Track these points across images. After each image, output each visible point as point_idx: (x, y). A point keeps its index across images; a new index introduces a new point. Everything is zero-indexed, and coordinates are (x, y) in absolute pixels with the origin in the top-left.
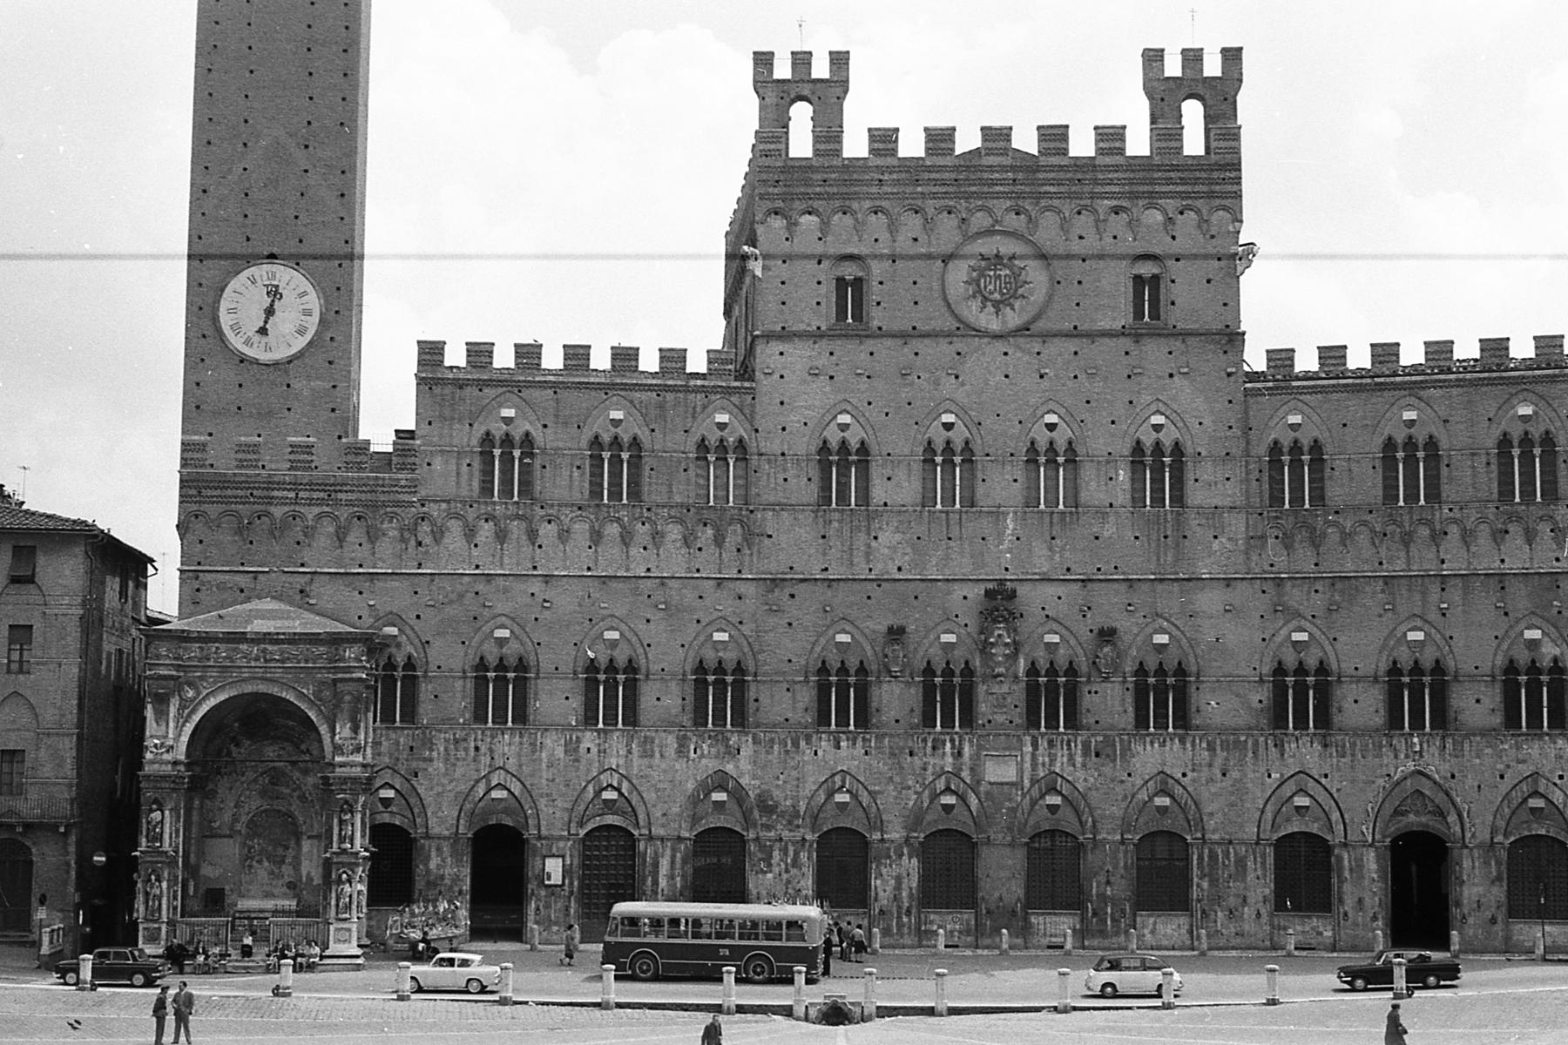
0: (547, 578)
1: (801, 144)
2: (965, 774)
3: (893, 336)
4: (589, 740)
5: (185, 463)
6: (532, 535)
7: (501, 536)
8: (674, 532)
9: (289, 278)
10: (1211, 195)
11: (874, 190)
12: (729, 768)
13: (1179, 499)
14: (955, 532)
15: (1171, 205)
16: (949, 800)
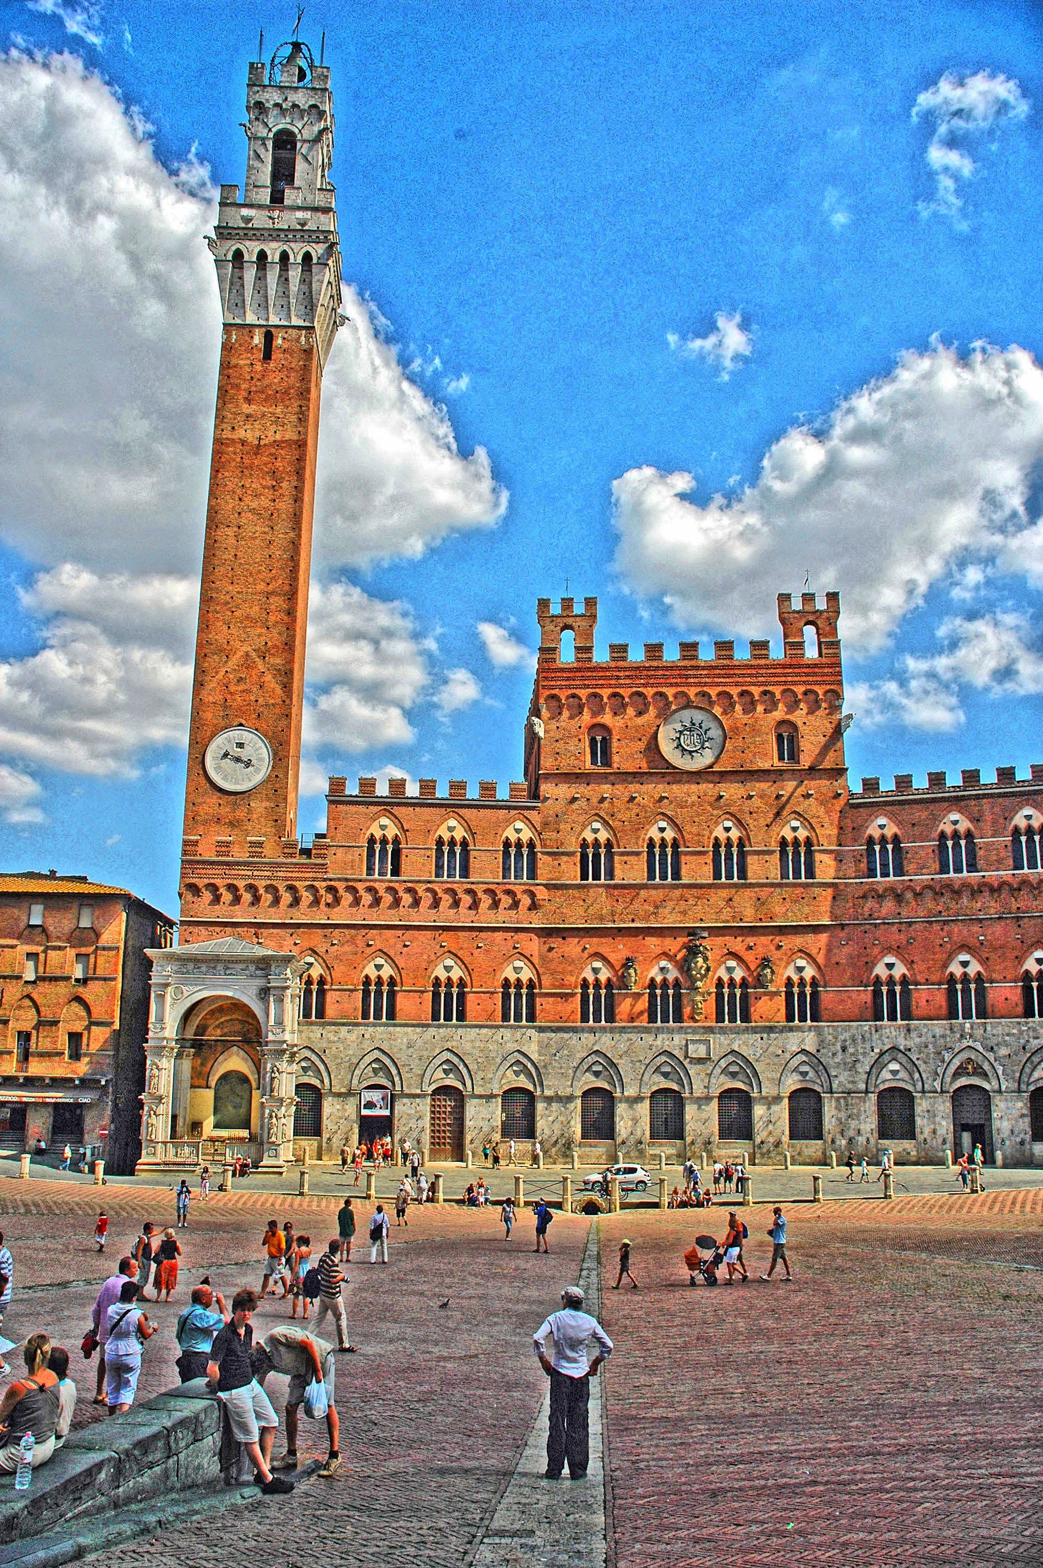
1: (567, 655)
5: (185, 853)
11: (613, 682)
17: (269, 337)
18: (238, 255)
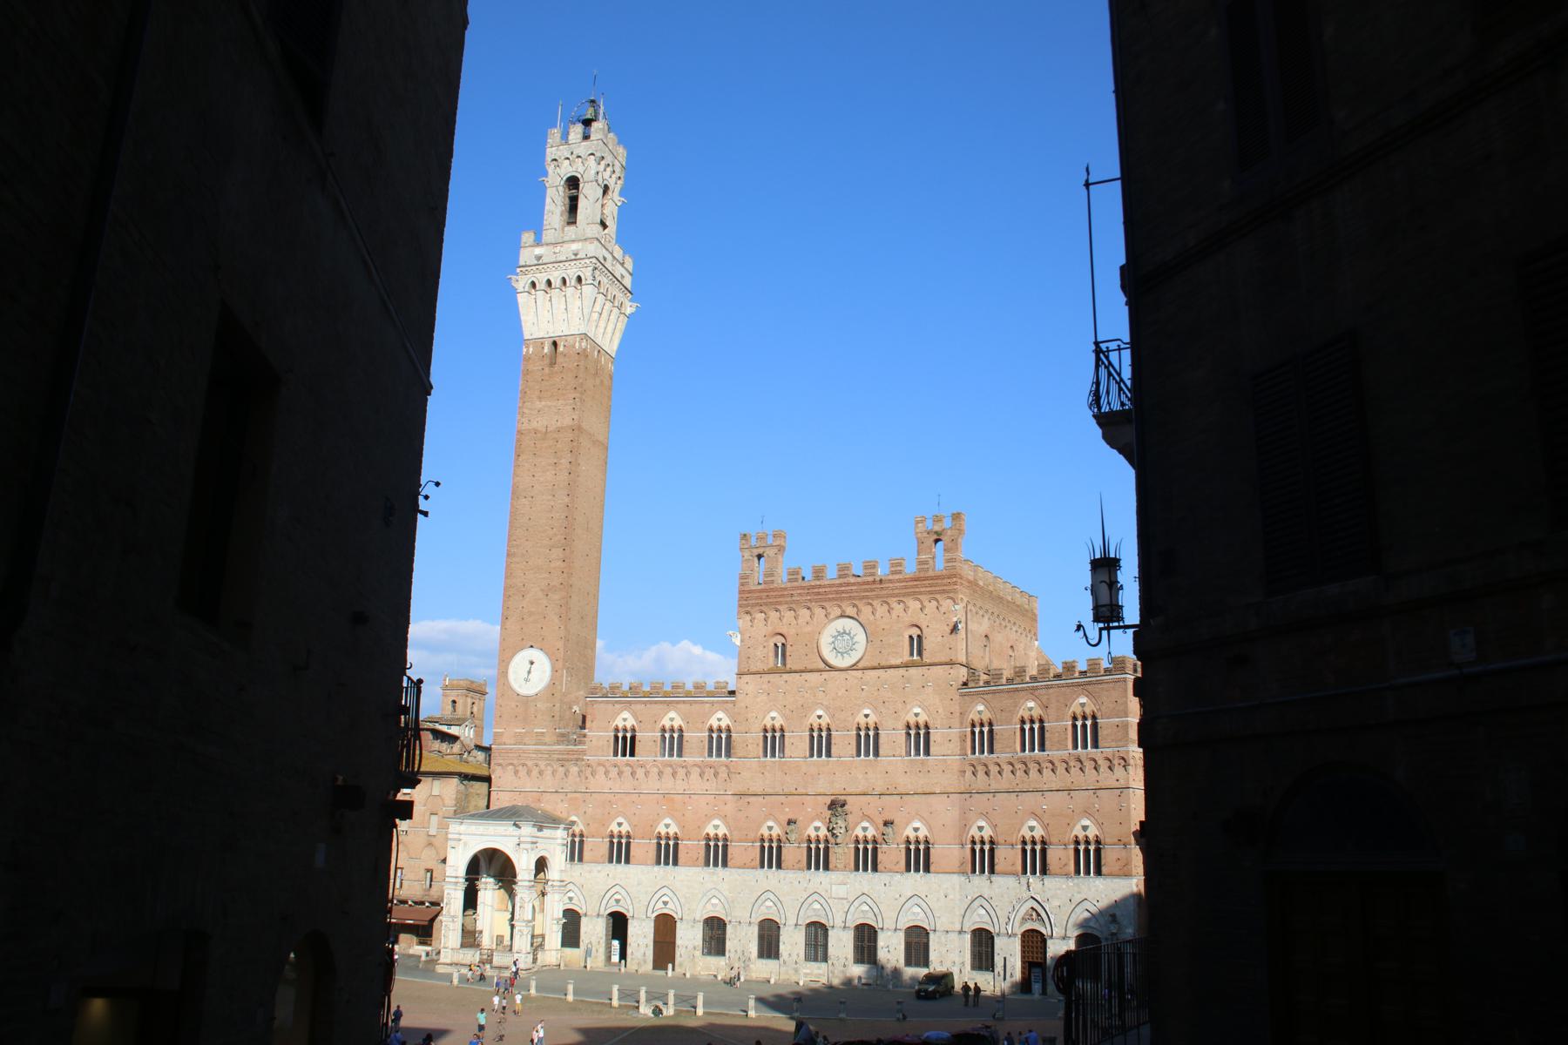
10: (944, 591)
13: (927, 753)
17: (555, 344)
18: (533, 285)
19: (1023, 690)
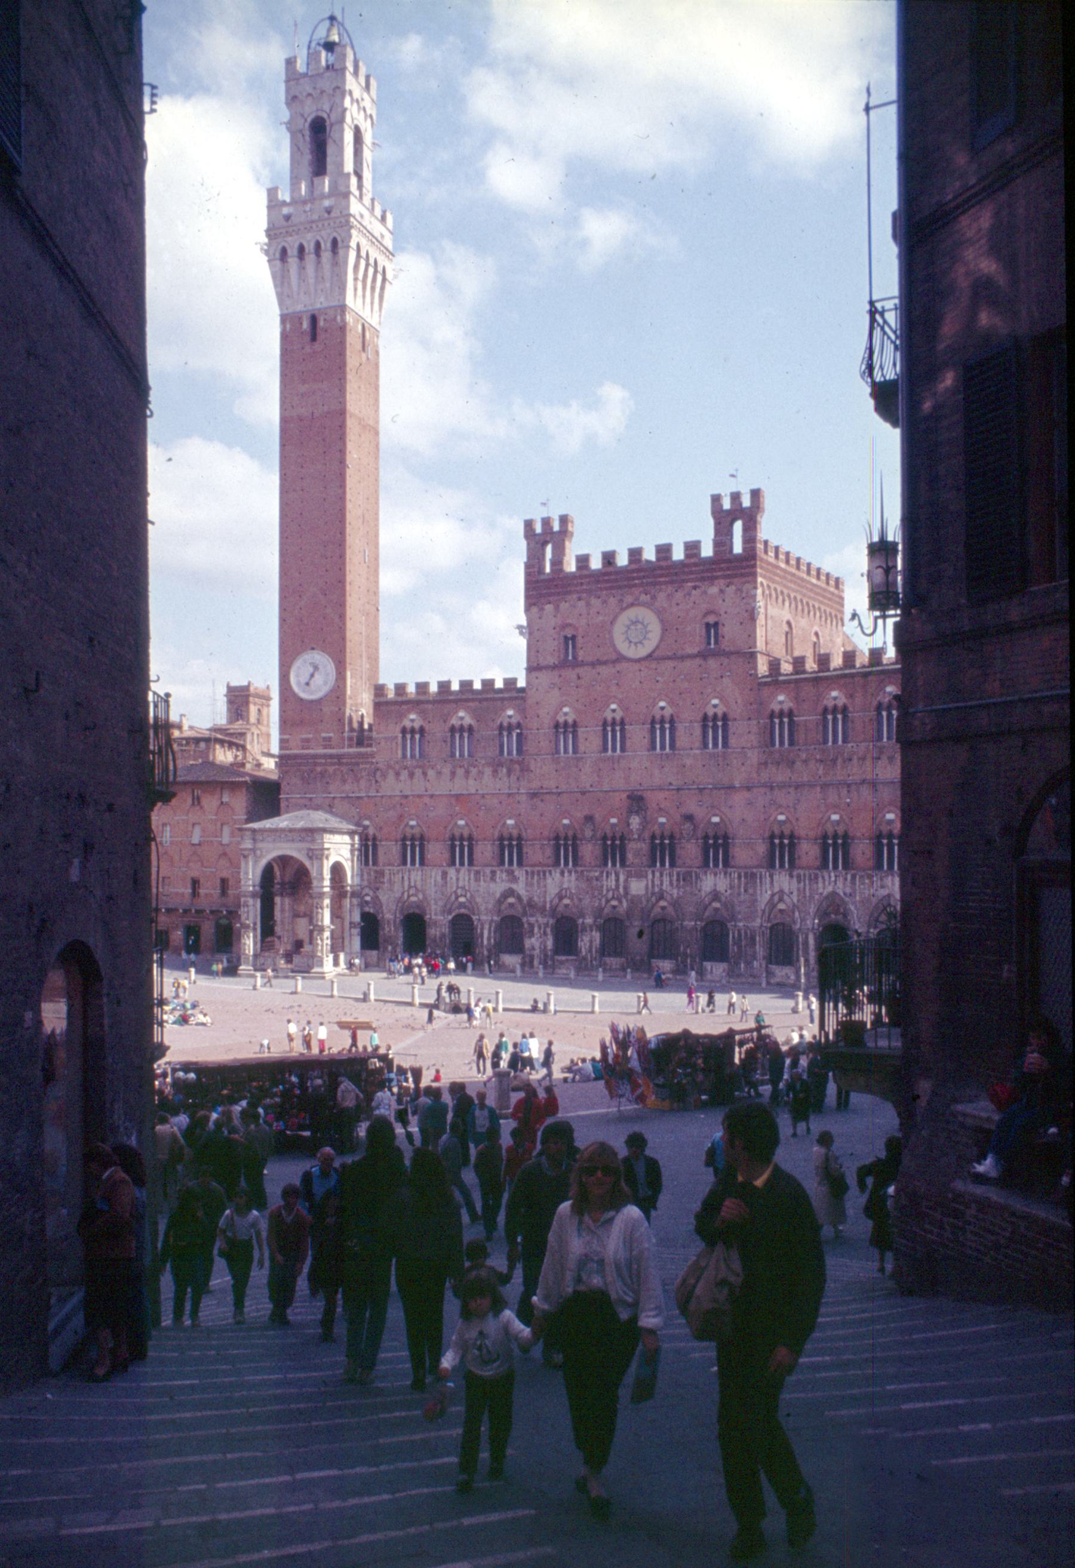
0: (432, 796)
2: (621, 890)
3: (588, 664)
4: (452, 872)
6: (425, 774)
7: (411, 775)
8: (488, 771)
9: (319, 657)
12: (514, 886)
13: (725, 744)
14: (616, 766)
15: (722, 582)
16: (614, 903)
17: (314, 320)
18: (284, 252)
19: (827, 678)
